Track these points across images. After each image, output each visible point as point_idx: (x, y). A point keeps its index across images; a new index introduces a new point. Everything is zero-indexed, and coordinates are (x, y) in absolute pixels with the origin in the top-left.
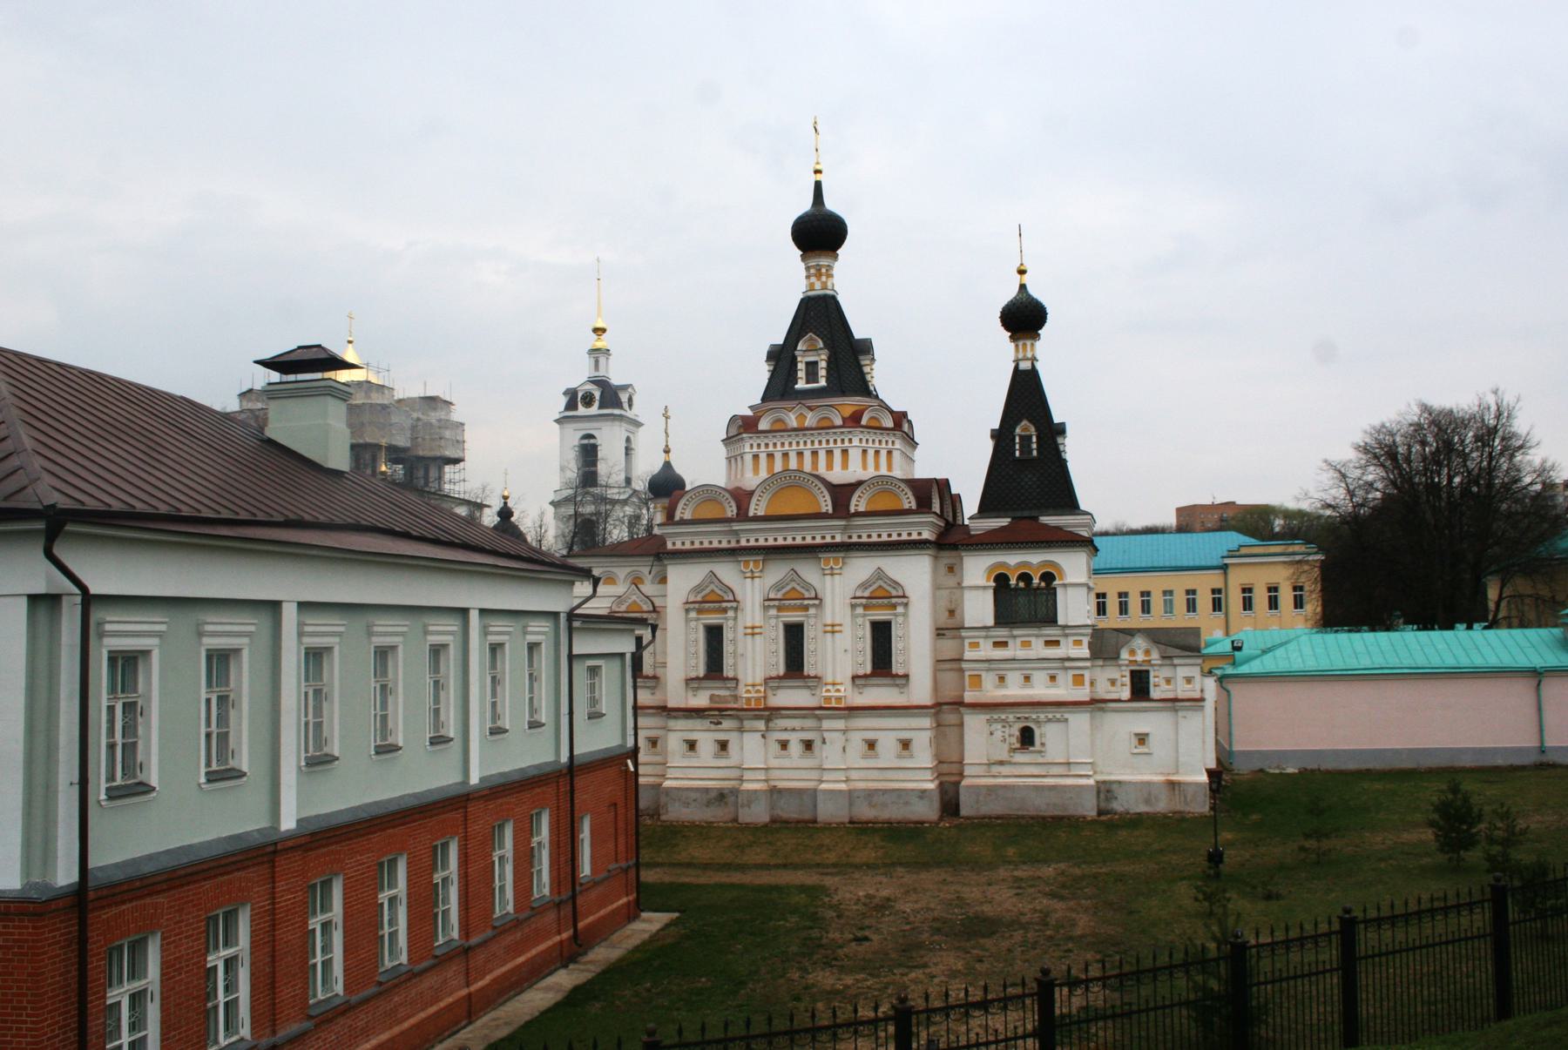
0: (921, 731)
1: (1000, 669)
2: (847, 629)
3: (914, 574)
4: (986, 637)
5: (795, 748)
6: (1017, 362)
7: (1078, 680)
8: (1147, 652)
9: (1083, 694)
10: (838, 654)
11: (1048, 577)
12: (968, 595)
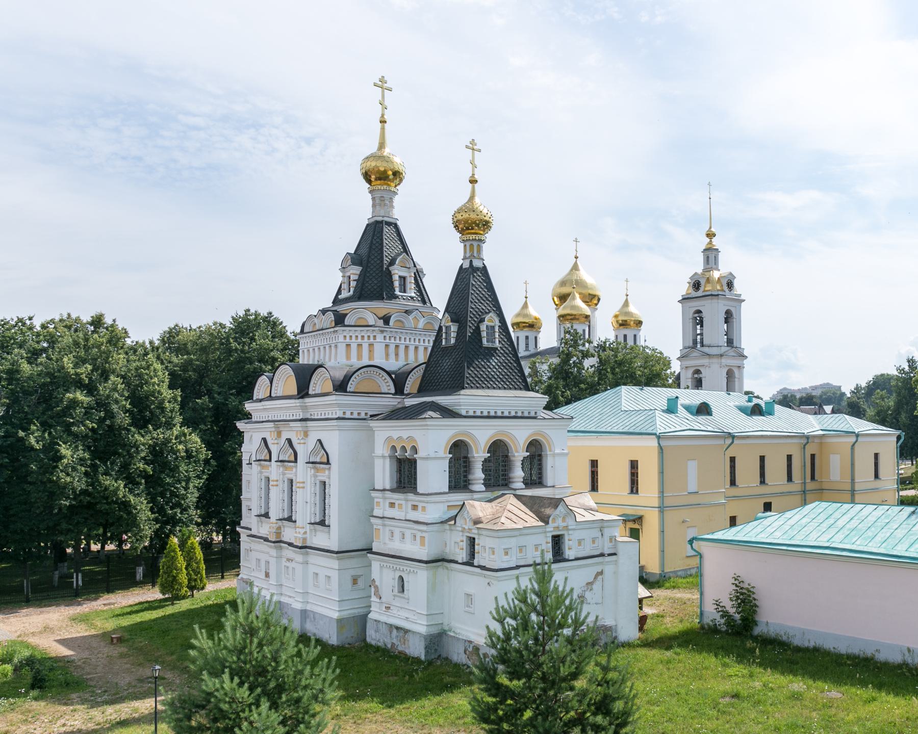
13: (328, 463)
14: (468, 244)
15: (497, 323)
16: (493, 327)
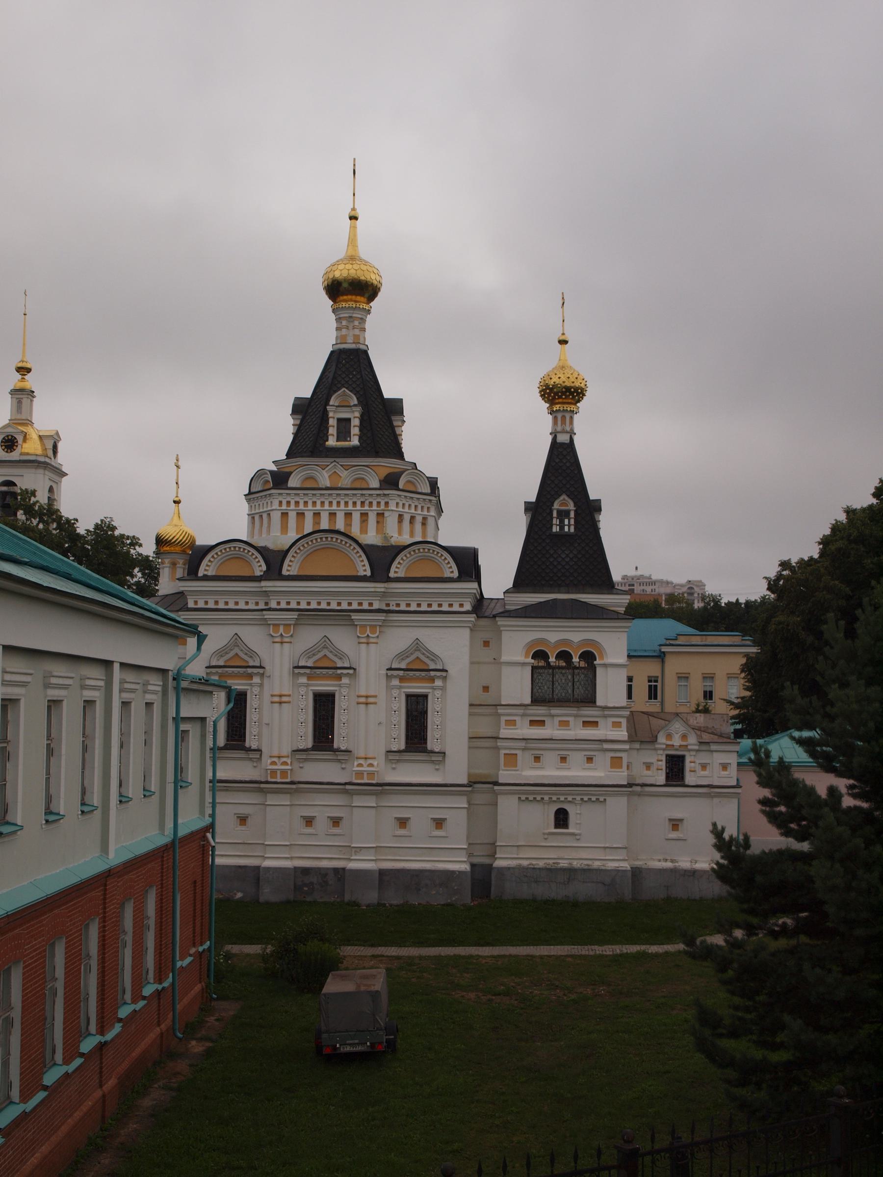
0: (455, 810)
1: (536, 750)
3: (452, 645)
4: (523, 715)
5: (322, 825)
6: (554, 434)
7: (616, 762)
8: (684, 737)
9: (620, 777)
10: (370, 727)
11: (588, 657)
12: (506, 671)
14: (559, 416)
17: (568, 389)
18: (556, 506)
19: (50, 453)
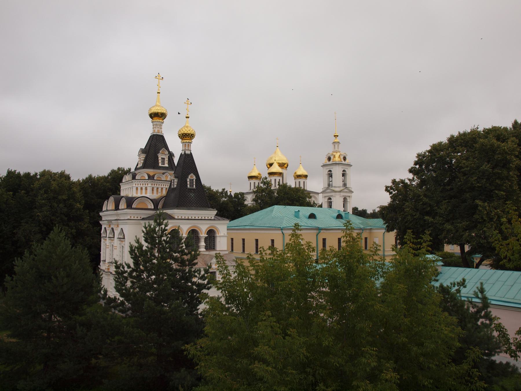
2: (118, 248)
13: (124, 238)
15: (194, 177)
16: (193, 180)
17: (189, 134)
18: (189, 176)
19: (342, 160)
